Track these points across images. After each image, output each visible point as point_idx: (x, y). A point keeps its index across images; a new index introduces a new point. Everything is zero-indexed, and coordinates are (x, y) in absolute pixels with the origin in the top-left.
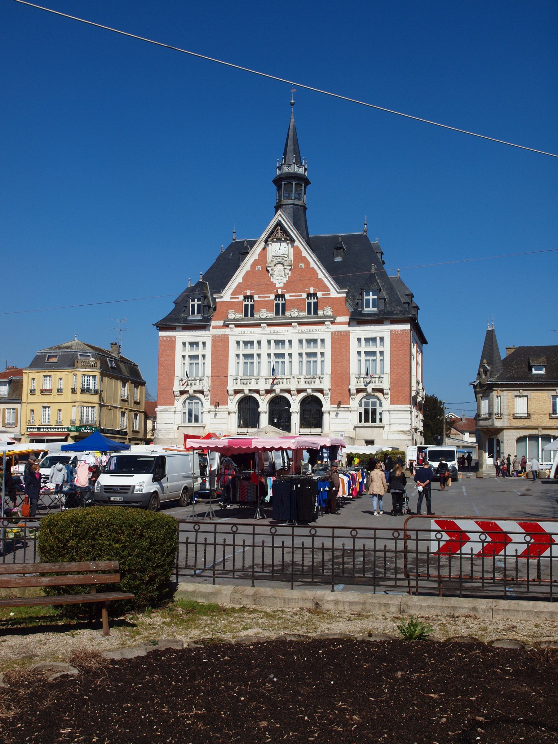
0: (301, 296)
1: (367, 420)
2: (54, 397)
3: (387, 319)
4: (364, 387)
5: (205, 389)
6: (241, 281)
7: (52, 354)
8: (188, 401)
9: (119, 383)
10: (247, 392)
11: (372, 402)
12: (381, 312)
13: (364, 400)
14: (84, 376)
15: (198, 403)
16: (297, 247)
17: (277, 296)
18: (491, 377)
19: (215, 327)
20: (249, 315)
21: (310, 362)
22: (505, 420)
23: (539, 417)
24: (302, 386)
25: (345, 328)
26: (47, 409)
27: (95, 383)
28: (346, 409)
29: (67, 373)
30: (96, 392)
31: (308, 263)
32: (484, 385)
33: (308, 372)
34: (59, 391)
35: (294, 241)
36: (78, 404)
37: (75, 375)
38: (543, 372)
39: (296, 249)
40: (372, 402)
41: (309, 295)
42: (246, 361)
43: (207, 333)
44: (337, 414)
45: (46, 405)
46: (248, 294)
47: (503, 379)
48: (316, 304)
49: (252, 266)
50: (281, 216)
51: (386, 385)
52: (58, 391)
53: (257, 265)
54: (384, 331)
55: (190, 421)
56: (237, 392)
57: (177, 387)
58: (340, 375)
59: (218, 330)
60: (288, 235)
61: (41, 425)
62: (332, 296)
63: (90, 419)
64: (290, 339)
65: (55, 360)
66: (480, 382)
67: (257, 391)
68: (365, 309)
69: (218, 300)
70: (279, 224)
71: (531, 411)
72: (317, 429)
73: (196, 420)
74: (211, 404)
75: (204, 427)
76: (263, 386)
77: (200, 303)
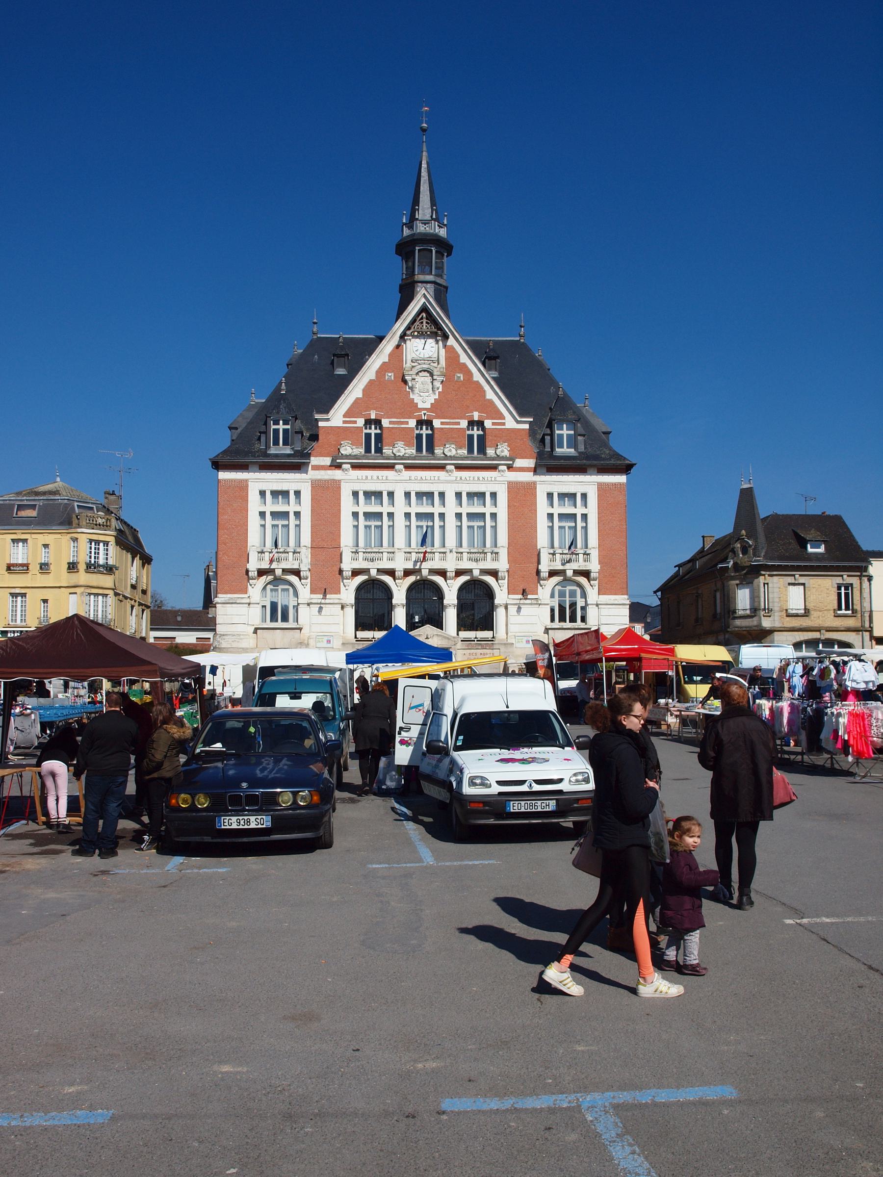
0: (458, 424)
1: (562, 619)
2: (34, 578)
3: (591, 466)
4: (561, 568)
5: (305, 567)
6: (360, 395)
7: (25, 503)
8: (269, 587)
9: (129, 556)
10: (373, 573)
11: (570, 590)
12: (582, 455)
13: (558, 588)
14: (91, 541)
15: (288, 590)
16: (452, 347)
17: (420, 423)
18: (755, 555)
19: (316, 468)
20: (374, 450)
21: (370, 527)
22: (777, 618)
23: (821, 613)
24: (465, 565)
25: (528, 477)
26: (19, 598)
27: (112, 554)
28: (533, 602)
29: (59, 536)
30: (110, 570)
31: (469, 373)
32: (743, 568)
33: (471, 544)
34: (44, 567)
35: (446, 337)
36: (82, 589)
37: (75, 540)
38: (822, 550)
39: (450, 351)
40: (570, 590)
41: (471, 423)
42: (368, 523)
43: (303, 476)
44: (519, 609)
45: (17, 591)
46: (373, 417)
47: (772, 559)
48: (482, 440)
49: (377, 372)
50: (425, 296)
51: (594, 566)
52: (41, 568)
53: (386, 371)
54: (587, 484)
55: (274, 618)
56: (355, 573)
57: (253, 565)
58: (524, 550)
59: (322, 472)
60: (440, 328)
61: (9, 626)
62: (507, 426)
63: (100, 616)
64: (441, 490)
65: (33, 513)
66: (735, 564)
67: (391, 573)
68: (557, 450)
69: (321, 424)
70: (424, 309)
71: (810, 606)
72: (486, 632)
73: (285, 618)
74: (313, 591)
75: (300, 629)
76: (400, 564)
77: (288, 427)
